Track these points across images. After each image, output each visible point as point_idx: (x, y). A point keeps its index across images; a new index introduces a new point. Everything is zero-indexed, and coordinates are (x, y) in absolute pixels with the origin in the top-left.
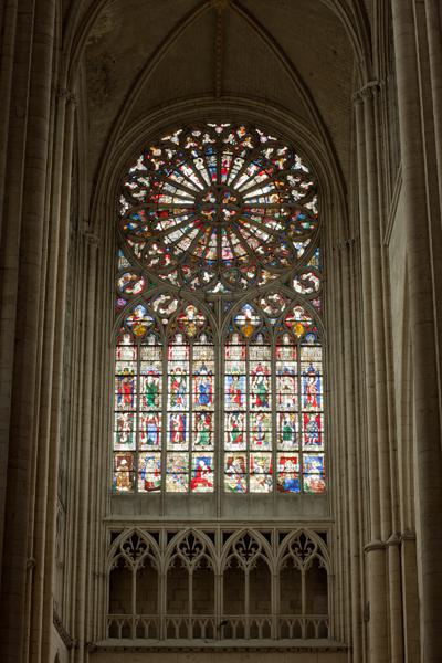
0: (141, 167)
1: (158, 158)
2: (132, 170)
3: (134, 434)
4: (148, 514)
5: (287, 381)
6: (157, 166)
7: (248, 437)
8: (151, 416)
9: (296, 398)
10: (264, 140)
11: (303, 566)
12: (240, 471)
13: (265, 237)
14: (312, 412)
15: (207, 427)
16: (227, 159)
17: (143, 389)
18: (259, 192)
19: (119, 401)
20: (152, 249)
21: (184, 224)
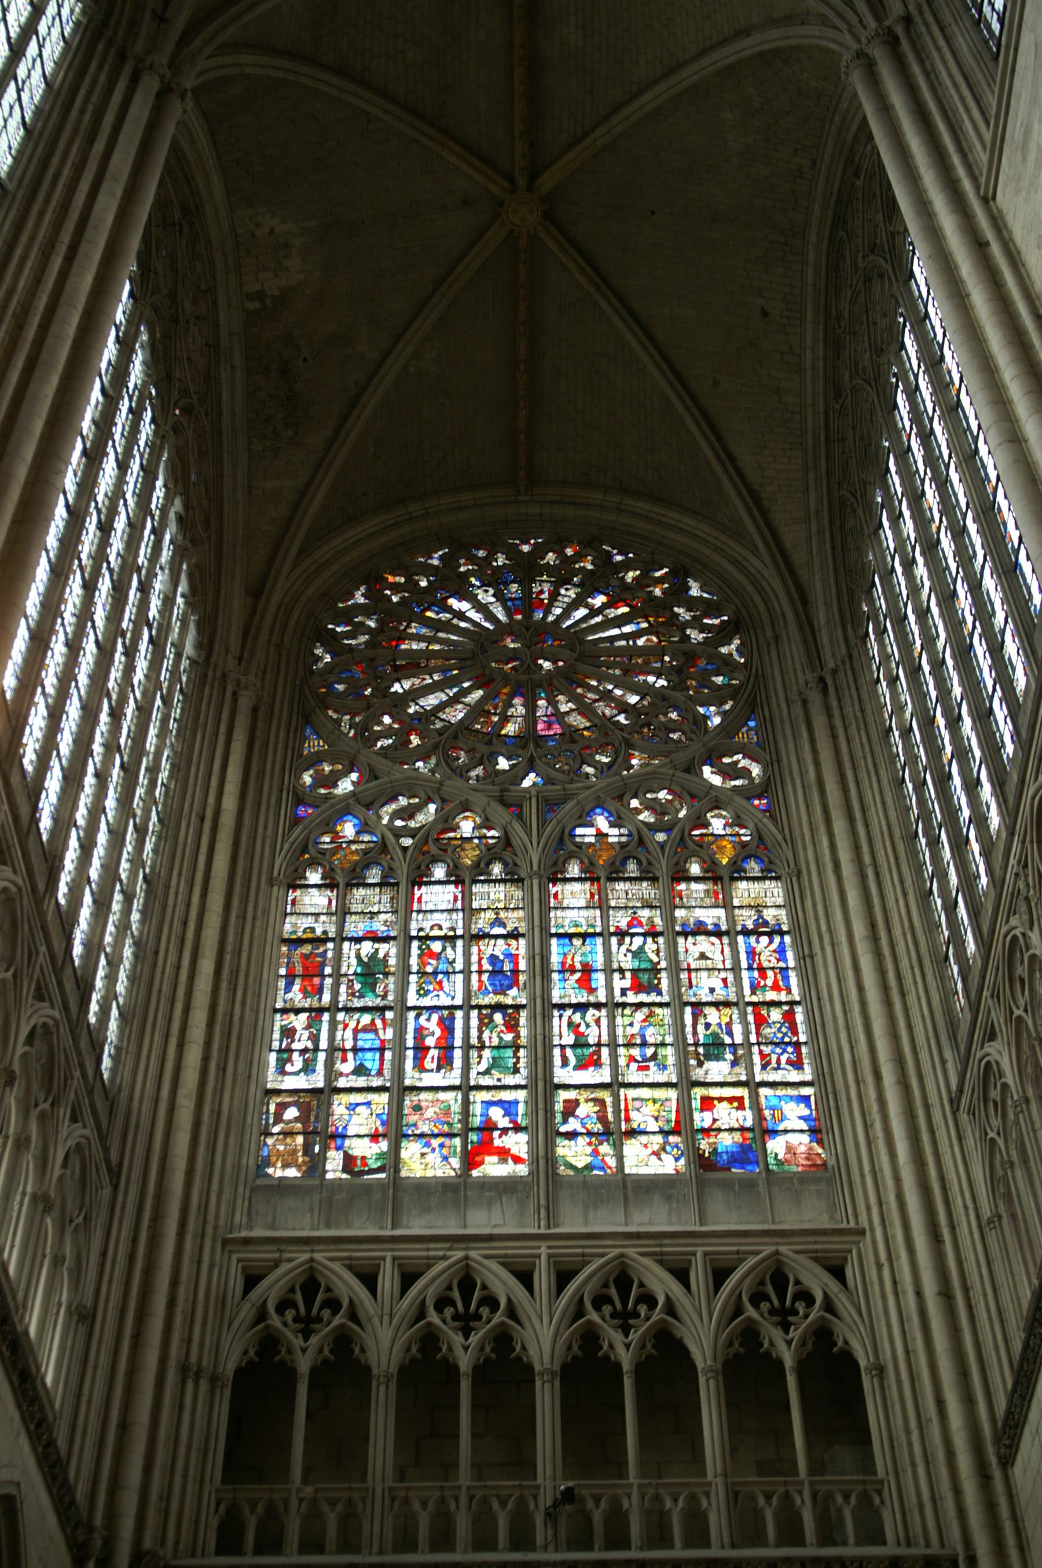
1: (396, 588)
3: (322, 1056)
4: (349, 1226)
5: (704, 944)
6: (395, 599)
7: (614, 1057)
8: (366, 1019)
9: (730, 977)
12: (598, 1127)
13: (633, 699)
15: (508, 1037)
16: (543, 588)
17: (350, 965)
19: (288, 989)
20: (381, 723)
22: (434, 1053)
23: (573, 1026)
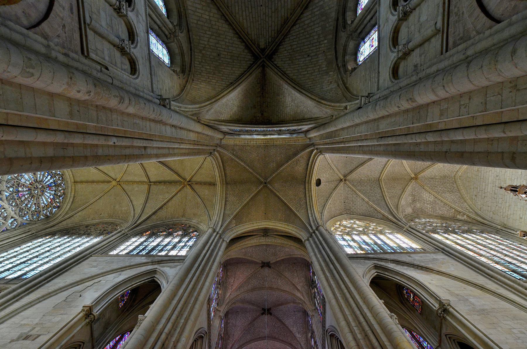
10: (61, 198)
13: (29, 206)
18: (44, 200)
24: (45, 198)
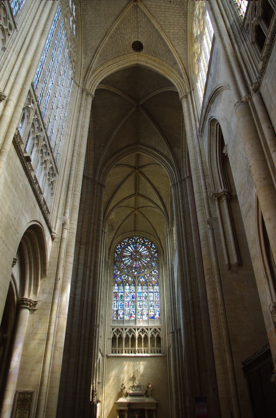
0: (119, 247)
1: (123, 245)
2: (117, 247)
8: (121, 302)
10: (146, 241)
11: (156, 336)
13: (146, 262)
14: (157, 301)
17: (120, 296)
18: (145, 252)
21: (129, 259)
22: (127, 306)
23: (139, 303)
24: (143, 251)
